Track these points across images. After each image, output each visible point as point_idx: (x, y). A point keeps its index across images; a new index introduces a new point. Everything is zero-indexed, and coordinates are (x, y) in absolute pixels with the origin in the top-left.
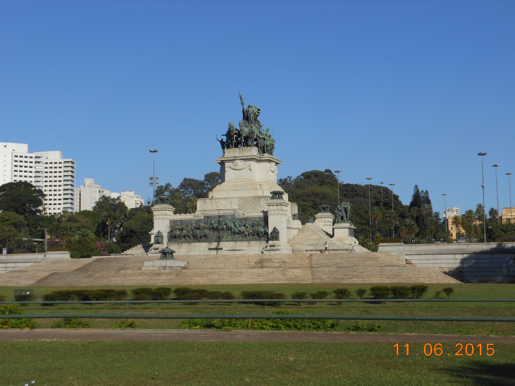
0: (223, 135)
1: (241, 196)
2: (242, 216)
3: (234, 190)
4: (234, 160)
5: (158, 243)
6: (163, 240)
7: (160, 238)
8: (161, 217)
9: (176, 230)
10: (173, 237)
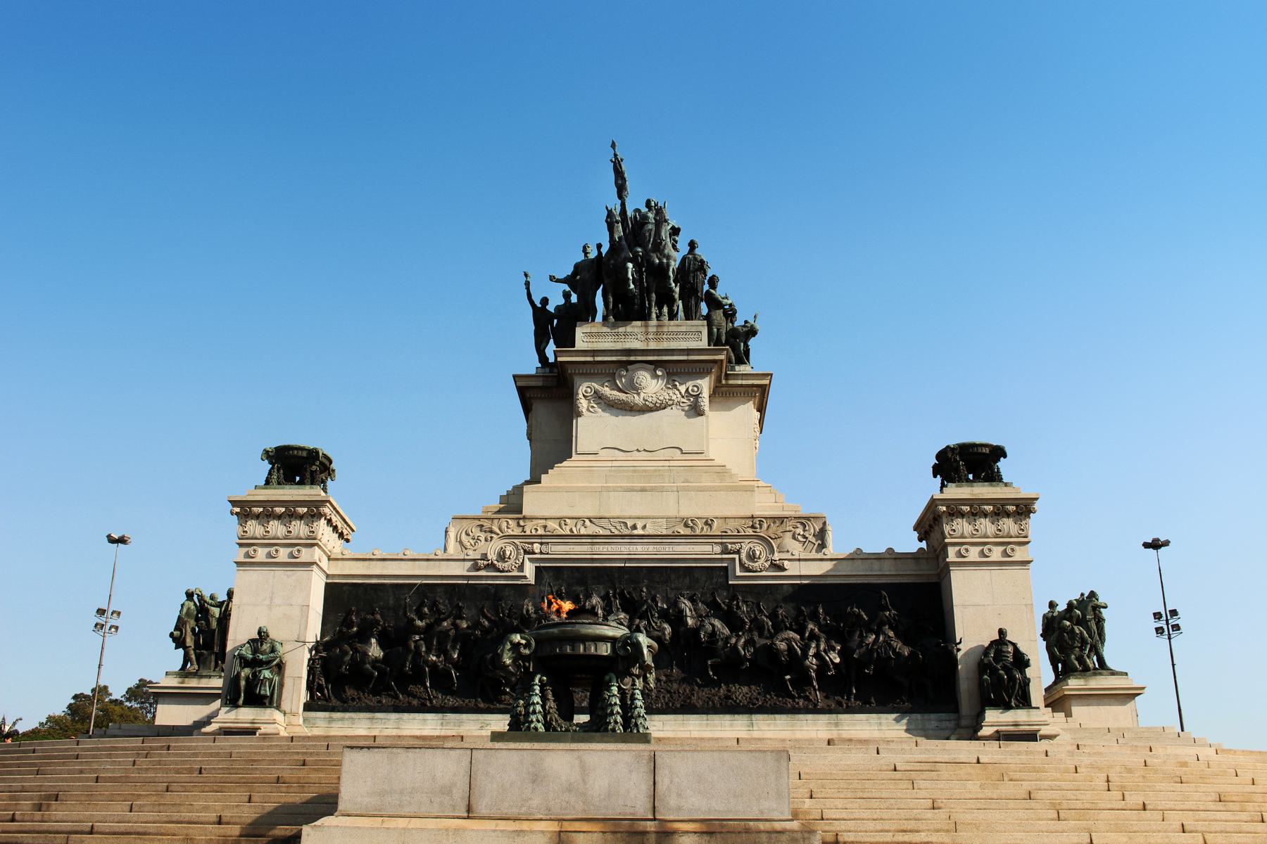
0: (552, 278)
1: (672, 512)
2: (766, 576)
3: (631, 490)
4: (625, 365)
5: (255, 700)
6: (281, 685)
7: (267, 673)
8: (283, 555)
9: (363, 637)
10: (341, 679)
